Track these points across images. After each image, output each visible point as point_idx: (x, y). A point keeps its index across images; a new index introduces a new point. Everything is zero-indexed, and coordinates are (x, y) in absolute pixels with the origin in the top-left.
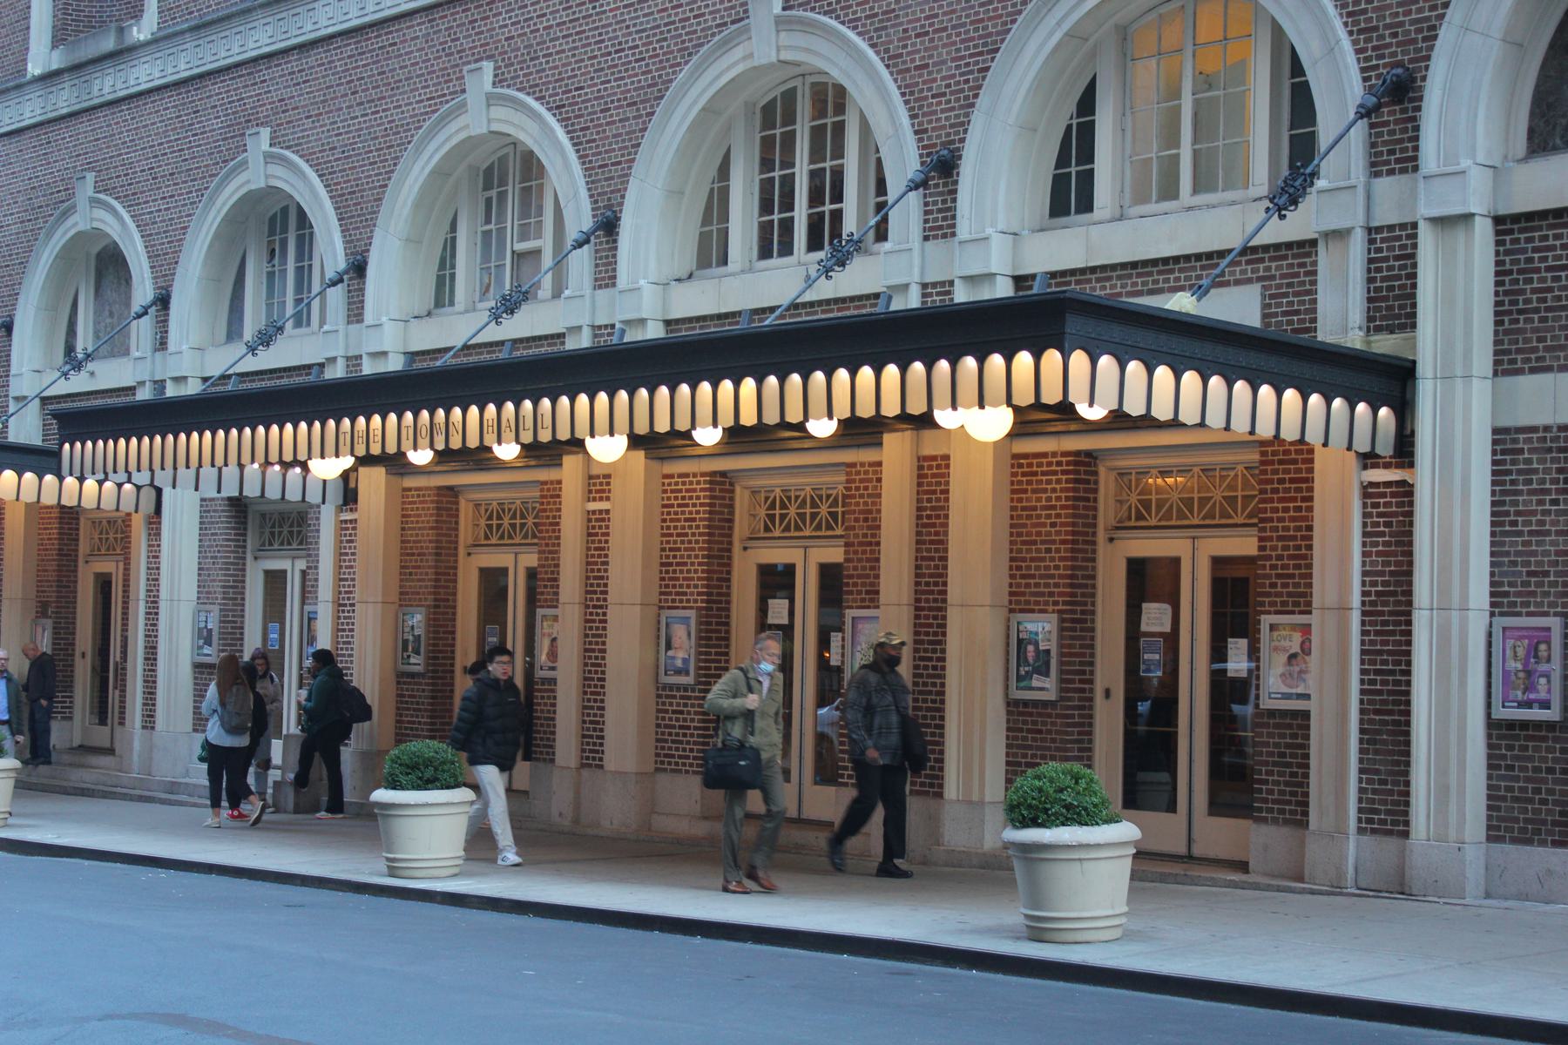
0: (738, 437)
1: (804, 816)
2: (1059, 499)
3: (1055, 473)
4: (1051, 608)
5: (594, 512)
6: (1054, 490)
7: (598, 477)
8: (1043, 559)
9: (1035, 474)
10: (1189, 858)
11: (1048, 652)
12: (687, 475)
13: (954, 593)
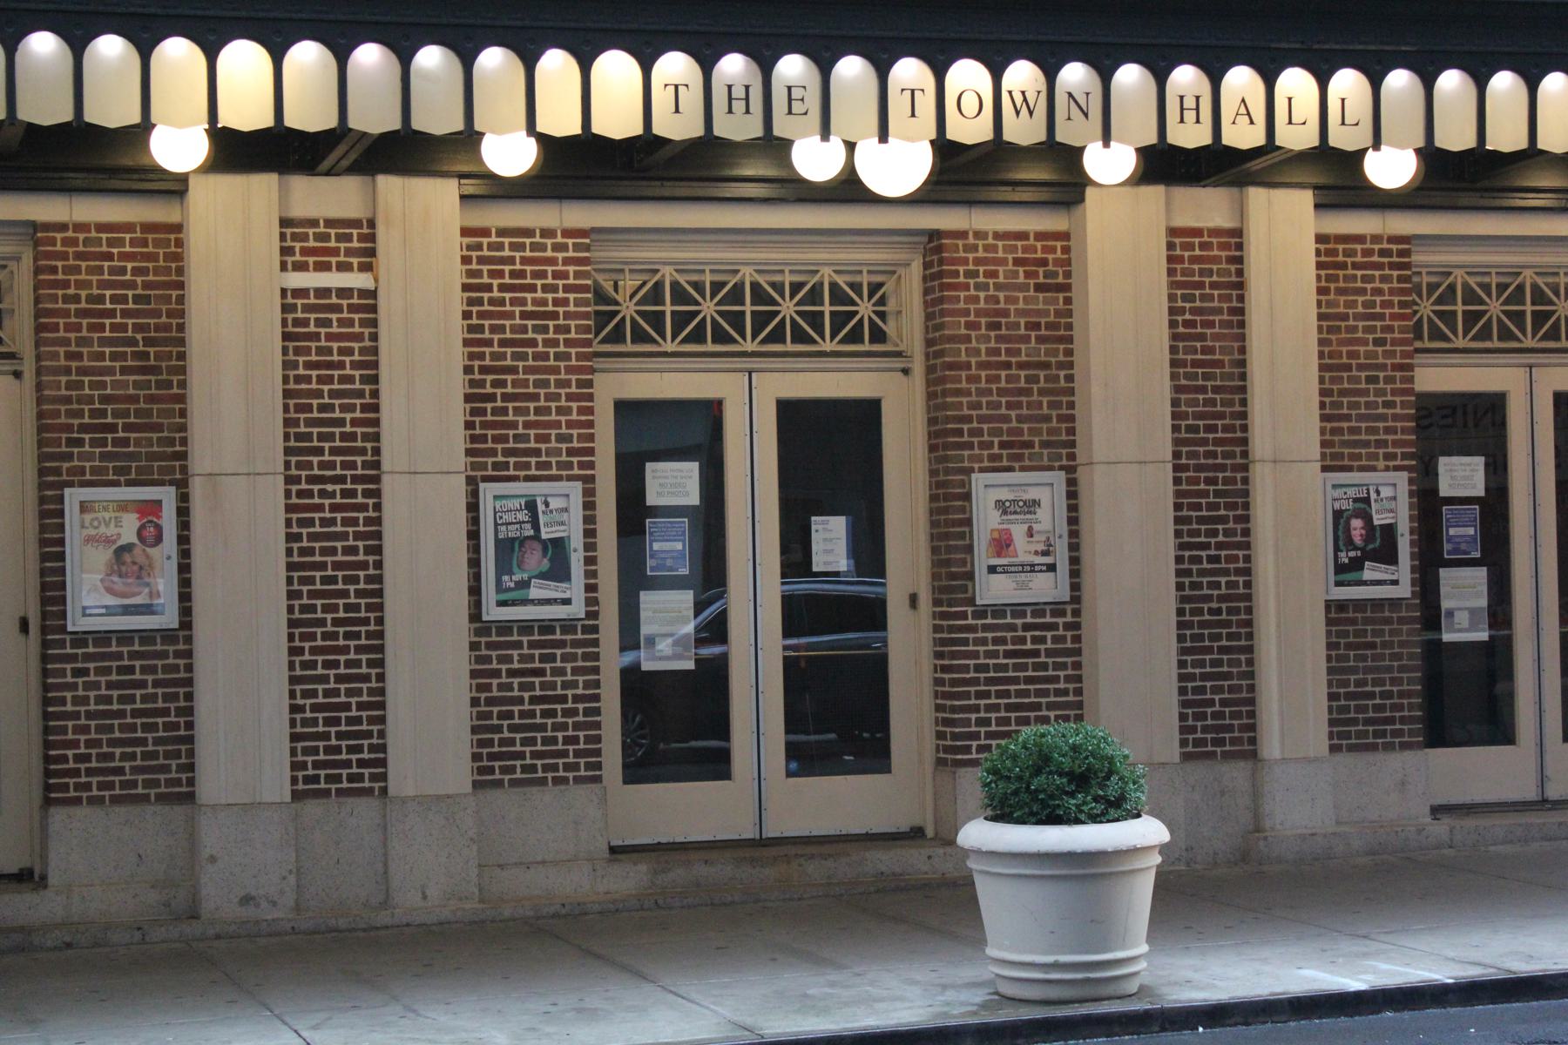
0: (580, 165)
1: (770, 832)
2: (1389, 304)
3: (1380, 266)
4: (1381, 464)
5: (300, 293)
6: (1379, 292)
7: (313, 223)
8: (1365, 393)
9: (1343, 266)
10: (1544, 804)
11: (1389, 531)
12: (528, 233)
13: (1261, 442)
